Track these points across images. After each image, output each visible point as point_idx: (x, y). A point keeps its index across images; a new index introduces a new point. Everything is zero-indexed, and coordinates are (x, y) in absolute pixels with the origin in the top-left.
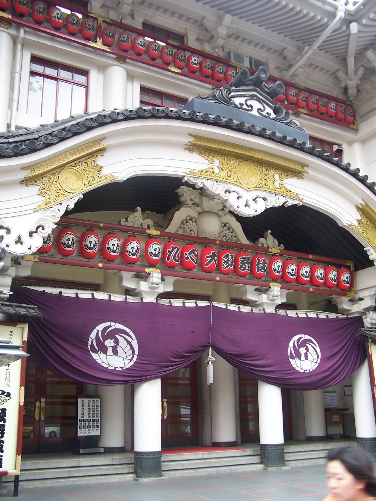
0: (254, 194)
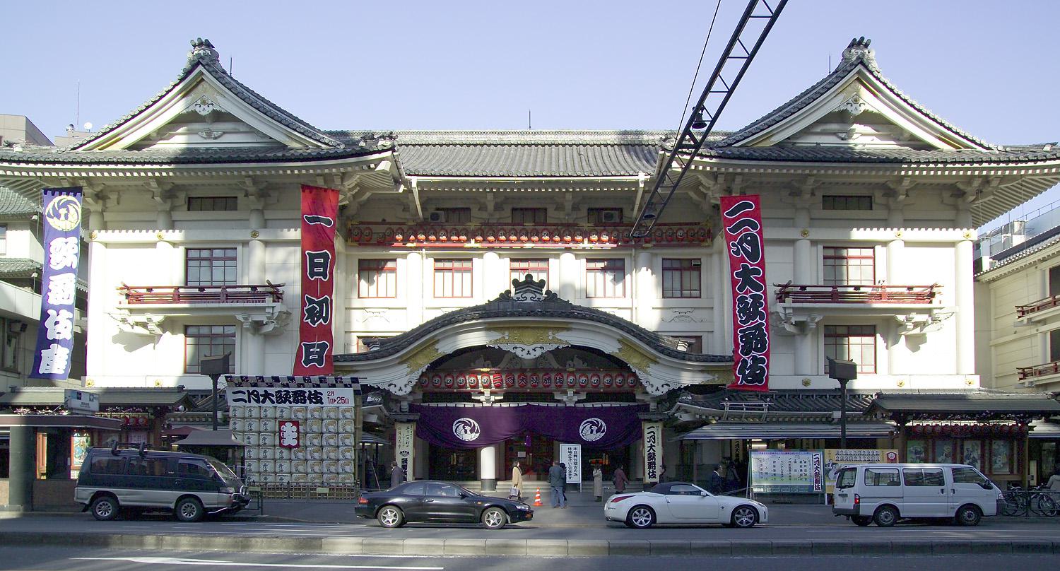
0: (534, 346)
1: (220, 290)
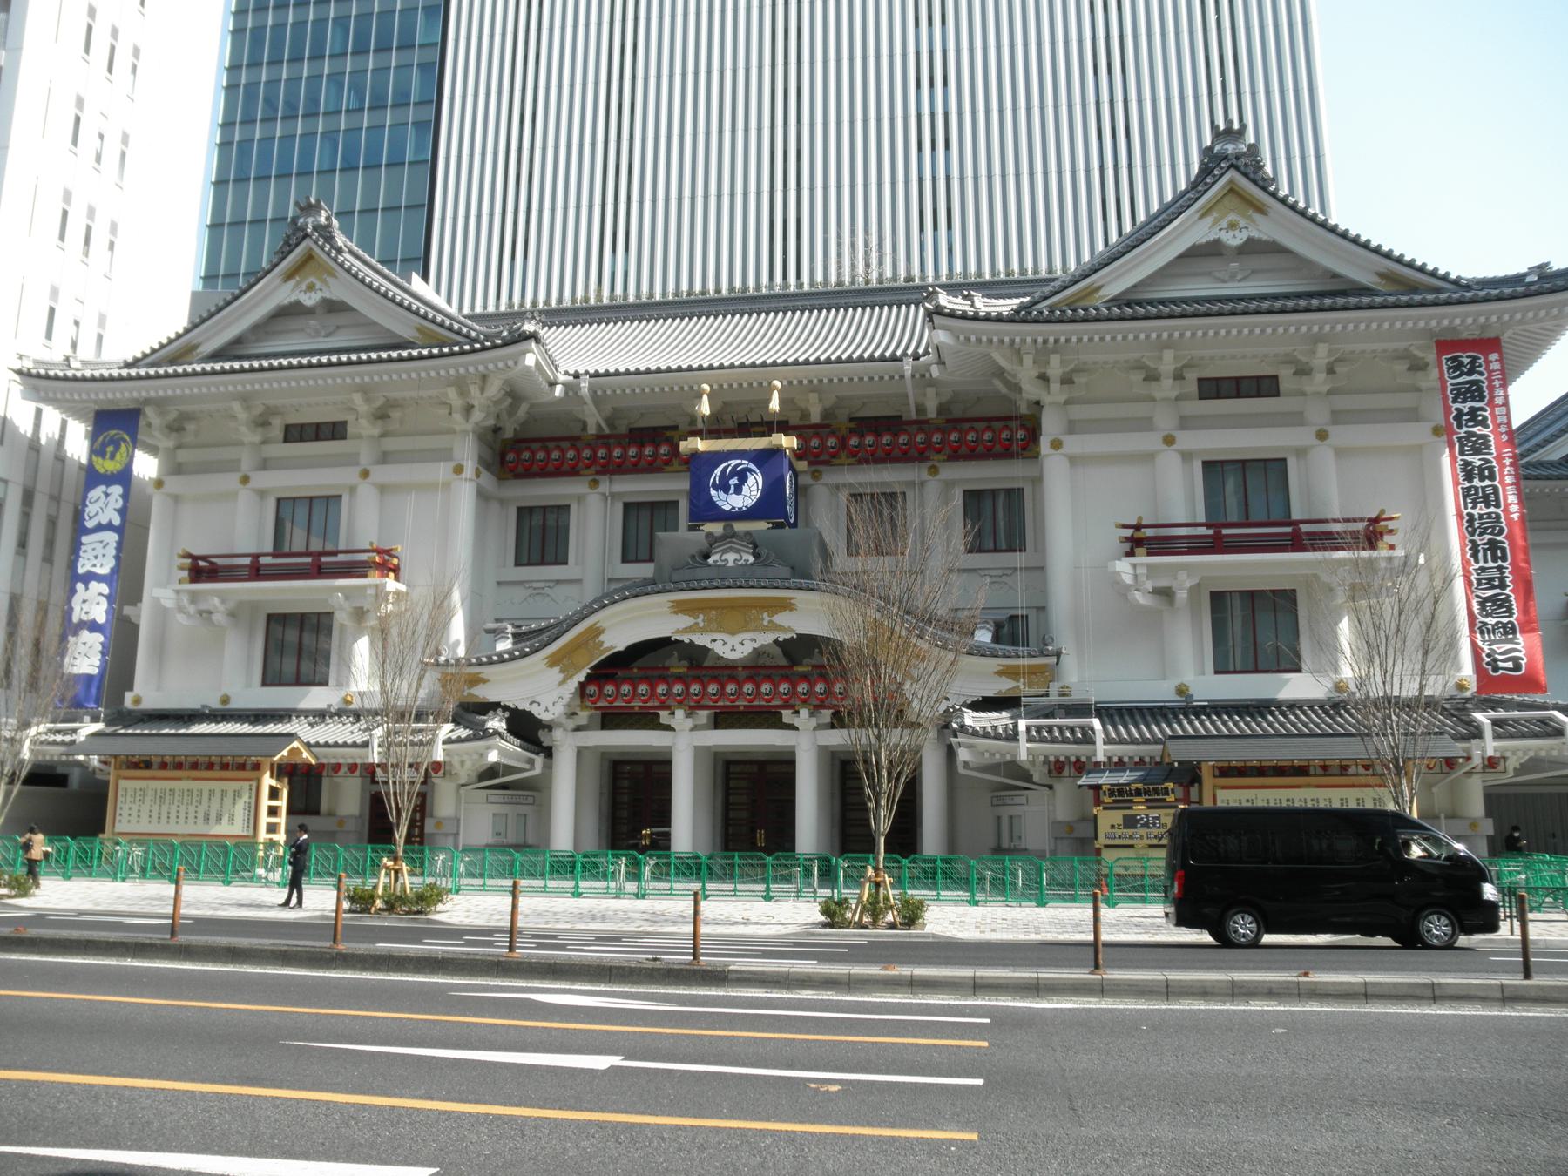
1: (309, 560)
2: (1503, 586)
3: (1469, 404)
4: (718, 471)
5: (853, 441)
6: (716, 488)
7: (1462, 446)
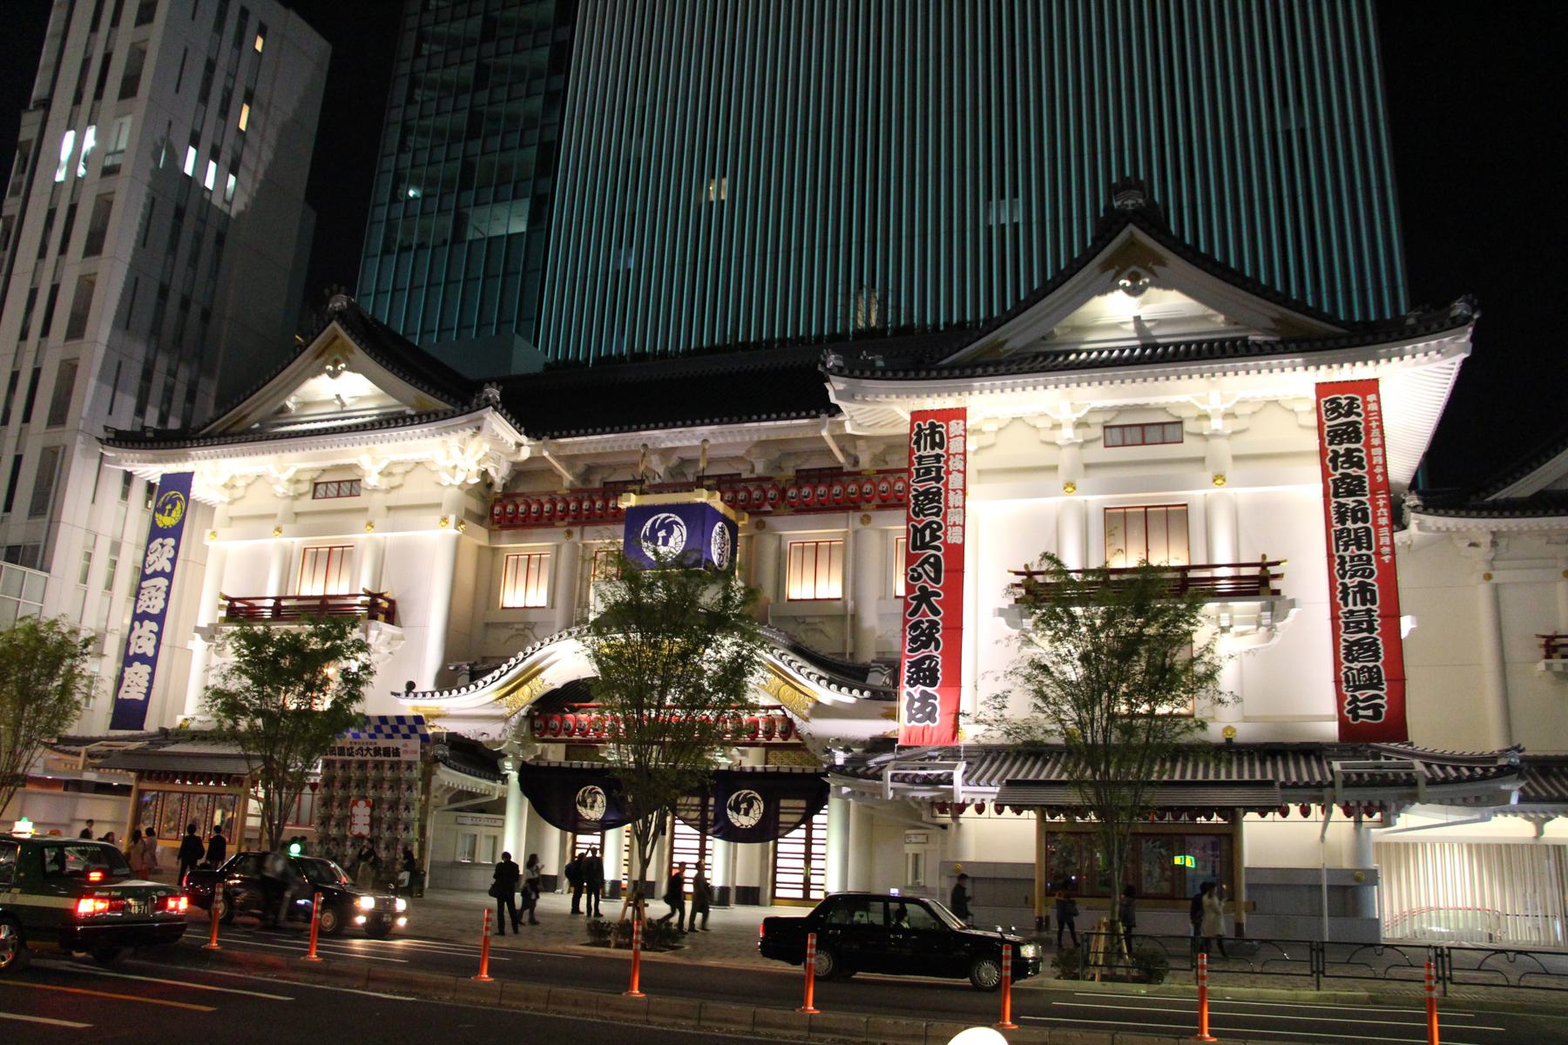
2: (1371, 629)
3: (1345, 446)
4: (649, 524)
5: (792, 492)
6: (646, 539)
7: (1336, 488)
